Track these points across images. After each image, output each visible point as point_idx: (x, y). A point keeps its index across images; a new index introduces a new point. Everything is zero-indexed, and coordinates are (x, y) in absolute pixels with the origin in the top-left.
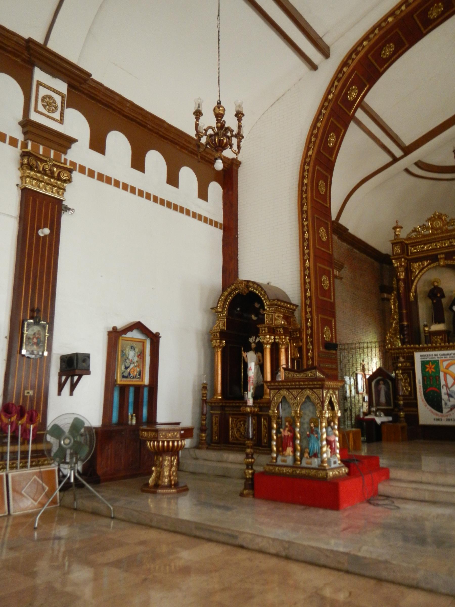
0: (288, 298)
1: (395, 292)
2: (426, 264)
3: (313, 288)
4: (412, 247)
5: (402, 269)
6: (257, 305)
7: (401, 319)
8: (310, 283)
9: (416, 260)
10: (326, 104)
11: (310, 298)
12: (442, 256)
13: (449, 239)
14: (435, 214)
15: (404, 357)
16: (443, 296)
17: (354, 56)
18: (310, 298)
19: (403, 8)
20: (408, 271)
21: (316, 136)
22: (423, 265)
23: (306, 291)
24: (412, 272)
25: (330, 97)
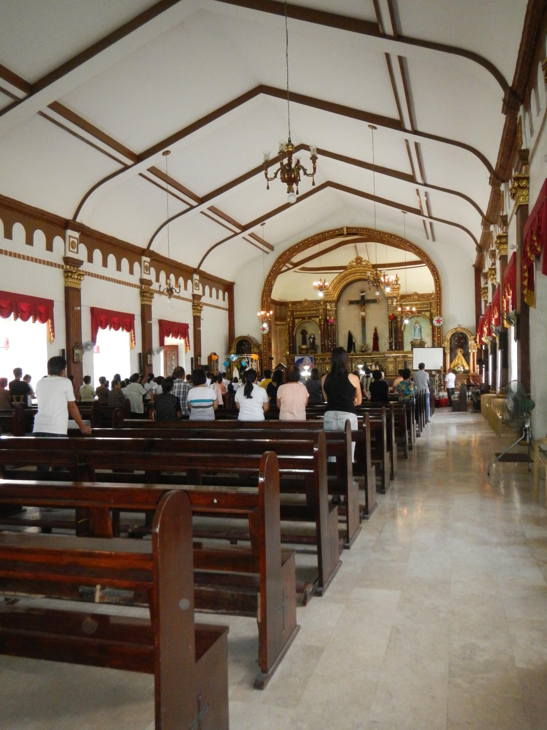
0: (257, 341)
1: (288, 331)
2: (300, 320)
3: (266, 339)
4: (295, 312)
5: (291, 322)
6: (245, 343)
7: (289, 343)
8: (265, 337)
9: (297, 318)
10: (273, 271)
11: (265, 342)
12: (307, 318)
13: (310, 311)
14: (305, 299)
15: (291, 359)
16: (306, 334)
17: (283, 256)
18: (265, 342)
19: (301, 244)
20: (293, 322)
21: (268, 282)
22: (299, 320)
23: (264, 339)
24: (295, 323)
25: (274, 269)
